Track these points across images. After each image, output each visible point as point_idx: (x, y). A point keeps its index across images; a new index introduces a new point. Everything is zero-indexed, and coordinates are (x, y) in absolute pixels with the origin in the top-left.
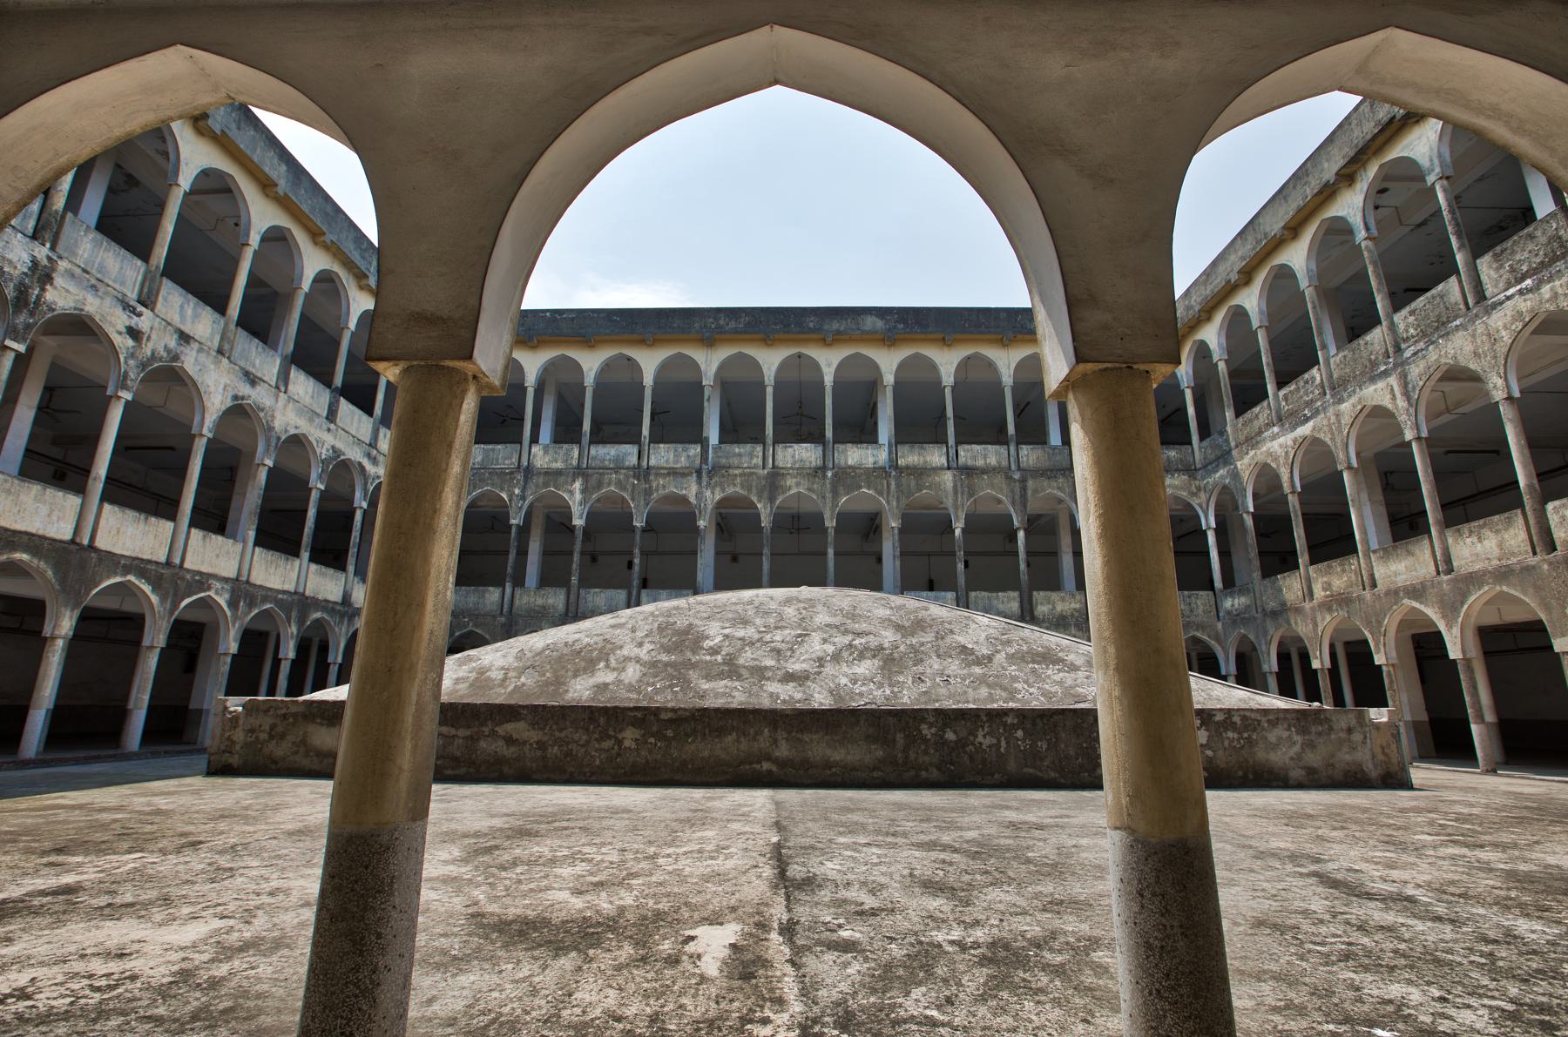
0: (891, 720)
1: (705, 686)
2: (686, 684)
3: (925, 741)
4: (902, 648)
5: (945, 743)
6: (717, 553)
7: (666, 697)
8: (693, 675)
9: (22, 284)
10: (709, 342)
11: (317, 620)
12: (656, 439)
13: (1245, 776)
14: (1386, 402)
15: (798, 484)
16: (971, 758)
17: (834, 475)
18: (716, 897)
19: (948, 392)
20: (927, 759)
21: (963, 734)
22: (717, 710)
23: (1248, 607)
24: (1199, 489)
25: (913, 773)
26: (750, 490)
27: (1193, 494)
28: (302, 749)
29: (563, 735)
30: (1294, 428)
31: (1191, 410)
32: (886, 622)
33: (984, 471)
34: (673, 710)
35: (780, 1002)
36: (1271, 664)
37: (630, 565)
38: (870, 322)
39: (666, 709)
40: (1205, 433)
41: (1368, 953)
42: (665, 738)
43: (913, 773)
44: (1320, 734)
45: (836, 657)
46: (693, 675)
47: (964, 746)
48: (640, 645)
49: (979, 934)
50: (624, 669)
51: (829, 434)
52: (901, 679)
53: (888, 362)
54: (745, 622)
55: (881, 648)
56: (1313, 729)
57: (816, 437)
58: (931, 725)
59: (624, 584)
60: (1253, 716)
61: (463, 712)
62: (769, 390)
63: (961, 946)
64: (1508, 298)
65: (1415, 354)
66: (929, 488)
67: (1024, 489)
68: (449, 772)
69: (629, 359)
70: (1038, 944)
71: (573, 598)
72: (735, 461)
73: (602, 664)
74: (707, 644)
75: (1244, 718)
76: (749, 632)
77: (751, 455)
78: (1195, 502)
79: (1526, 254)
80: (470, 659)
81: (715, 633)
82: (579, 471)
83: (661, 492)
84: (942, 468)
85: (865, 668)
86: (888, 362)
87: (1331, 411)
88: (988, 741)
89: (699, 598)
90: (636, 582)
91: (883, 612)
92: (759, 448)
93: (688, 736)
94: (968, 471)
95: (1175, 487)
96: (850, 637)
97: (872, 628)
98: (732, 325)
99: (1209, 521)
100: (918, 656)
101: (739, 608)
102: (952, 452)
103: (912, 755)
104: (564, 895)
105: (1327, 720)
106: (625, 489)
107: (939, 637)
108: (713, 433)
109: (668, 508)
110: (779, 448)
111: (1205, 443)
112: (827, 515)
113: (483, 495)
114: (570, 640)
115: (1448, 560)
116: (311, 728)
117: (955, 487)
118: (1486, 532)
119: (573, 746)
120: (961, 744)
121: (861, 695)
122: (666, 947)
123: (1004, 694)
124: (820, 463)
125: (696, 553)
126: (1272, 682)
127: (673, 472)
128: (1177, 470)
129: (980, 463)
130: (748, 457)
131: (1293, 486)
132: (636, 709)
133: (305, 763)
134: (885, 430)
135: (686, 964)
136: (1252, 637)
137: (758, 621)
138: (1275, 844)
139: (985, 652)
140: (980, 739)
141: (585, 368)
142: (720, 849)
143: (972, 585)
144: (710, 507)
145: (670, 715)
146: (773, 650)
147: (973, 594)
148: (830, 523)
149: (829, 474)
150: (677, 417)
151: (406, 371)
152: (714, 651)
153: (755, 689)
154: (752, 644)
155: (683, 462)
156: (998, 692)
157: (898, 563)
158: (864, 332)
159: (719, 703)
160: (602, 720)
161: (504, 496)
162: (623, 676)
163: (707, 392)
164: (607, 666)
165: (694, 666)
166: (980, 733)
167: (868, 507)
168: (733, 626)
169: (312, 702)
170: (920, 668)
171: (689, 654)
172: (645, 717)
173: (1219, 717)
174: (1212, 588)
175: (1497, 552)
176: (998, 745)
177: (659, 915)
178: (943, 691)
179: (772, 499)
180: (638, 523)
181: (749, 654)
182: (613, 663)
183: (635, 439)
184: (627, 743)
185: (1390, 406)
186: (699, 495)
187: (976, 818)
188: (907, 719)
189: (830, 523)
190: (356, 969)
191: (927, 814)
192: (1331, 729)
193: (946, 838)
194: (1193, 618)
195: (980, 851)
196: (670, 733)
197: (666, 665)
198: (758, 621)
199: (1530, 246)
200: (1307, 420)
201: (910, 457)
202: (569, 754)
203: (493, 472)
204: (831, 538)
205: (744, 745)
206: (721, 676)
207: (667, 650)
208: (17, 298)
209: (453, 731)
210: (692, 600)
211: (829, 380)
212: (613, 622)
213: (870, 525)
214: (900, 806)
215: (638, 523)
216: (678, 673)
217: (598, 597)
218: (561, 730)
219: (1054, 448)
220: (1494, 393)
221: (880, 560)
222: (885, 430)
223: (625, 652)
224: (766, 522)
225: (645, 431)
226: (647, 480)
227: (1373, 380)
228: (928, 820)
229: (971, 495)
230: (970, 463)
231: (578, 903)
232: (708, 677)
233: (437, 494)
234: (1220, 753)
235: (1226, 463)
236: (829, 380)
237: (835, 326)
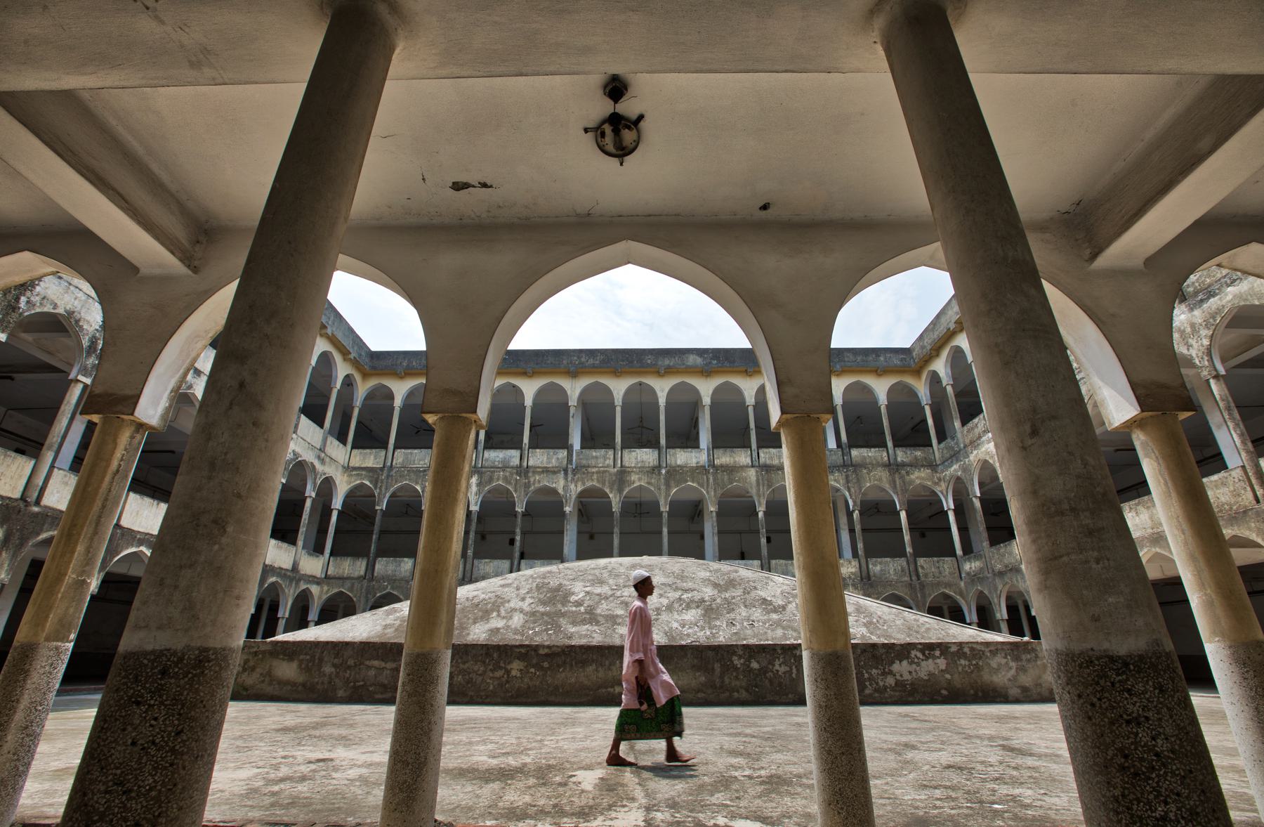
0: (710, 653)
1: (573, 629)
2: (558, 628)
3: (736, 669)
4: (719, 601)
5: (751, 670)
6: (579, 532)
7: (541, 636)
8: (563, 621)
9: (94, 337)
10: (574, 374)
11: (273, 583)
12: (534, 445)
13: (976, 694)
15: (640, 479)
16: (771, 681)
17: (667, 472)
18: (586, 758)
19: (751, 410)
20: (738, 683)
21: (764, 664)
22: (581, 647)
23: (981, 569)
24: (940, 480)
25: (727, 694)
26: (604, 484)
27: (936, 484)
28: (267, 679)
29: (466, 666)
31: (930, 422)
32: (706, 581)
34: (548, 647)
35: (633, 799)
36: (1002, 613)
37: (512, 542)
38: (692, 360)
39: (544, 647)
40: (942, 437)
41: (1012, 777)
42: (542, 668)
43: (727, 694)
44: (1029, 661)
45: (670, 608)
46: (563, 621)
47: (765, 673)
48: (523, 599)
49: (763, 773)
50: (511, 618)
51: (663, 441)
52: (718, 623)
53: (706, 388)
54: (601, 582)
55: (703, 601)
56: (1024, 657)
57: (653, 444)
58: (740, 657)
59: (509, 557)
60: (978, 647)
61: (391, 649)
62: (618, 409)
63: (750, 777)
66: (738, 481)
68: (379, 696)
69: (514, 386)
70: (799, 776)
71: (469, 566)
72: (593, 462)
73: (495, 614)
74: (573, 598)
75: (972, 649)
76: (604, 590)
77: (605, 458)
78: (937, 489)
80: (395, 611)
81: (579, 590)
84: (747, 466)
85: (691, 615)
86: (706, 388)
88: (783, 669)
89: (566, 565)
90: (517, 554)
91: (704, 574)
92: (611, 453)
93: (559, 666)
96: (679, 593)
97: (696, 586)
98: (591, 361)
99: (949, 504)
100: (730, 606)
101: (597, 572)
102: (755, 454)
103: (727, 680)
104: (485, 758)
105: (1034, 650)
106: (510, 483)
107: (746, 592)
108: (576, 440)
109: (542, 498)
110: (626, 452)
111: (942, 445)
112: (662, 502)
113: (401, 488)
114: (471, 595)
116: (275, 663)
117: (758, 481)
119: (473, 676)
120: (763, 671)
121: (688, 635)
122: (558, 779)
123: (795, 634)
124: (656, 463)
125: (562, 533)
126: (1004, 626)
127: (546, 471)
129: (776, 462)
130: (602, 459)
132: (521, 646)
133: (269, 690)
134: (705, 438)
135: (571, 785)
136: (986, 592)
137: (611, 582)
138: (982, 732)
139: (781, 603)
140: (777, 667)
142: (586, 737)
143: (772, 556)
144: (574, 497)
145: (546, 651)
146: (622, 603)
147: (773, 562)
148: (664, 508)
149: (663, 471)
150: (549, 431)
151: (441, 418)
152: (579, 604)
153: (609, 632)
154: (606, 598)
155: (554, 463)
156: (790, 632)
157: (716, 539)
158: (688, 367)
159: (583, 642)
160: (495, 655)
161: (418, 488)
162: (510, 623)
163: (572, 411)
164: (499, 615)
165: (563, 615)
166: (777, 663)
167: (693, 497)
168: (593, 585)
169: (277, 642)
170: (732, 615)
171: (559, 606)
172: (527, 653)
173: (954, 649)
174: (953, 554)
175: (1149, 523)
176: (790, 672)
177: (549, 767)
178: (749, 632)
179: (620, 491)
180: (520, 509)
181: (604, 606)
182: (503, 613)
183: (517, 445)
184: (514, 673)
187: (772, 721)
188: (722, 653)
189: (664, 508)
190: (422, 721)
191: (737, 719)
192: (1037, 657)
193: (748, 731)
194: (942, 579)
195: (769, 738)
196: (546, 665)
197: (543, 614)
198: (611, 582)
201: (723, 458)
202: (470, 681)
203: (411, 471)
205: (601, 674)
206: (584, 622)
207: (544, 603)
208: (90, 347)
209: (383, 665)
210: (561, 566)
211: (662, 401)
212: (503, 582)
213: (691, 512)
214: (717, 715)
215: (520, 509)
216: (552, 620)
217: (486, 565)
218: (464, 663)
219: (831, 450)
221: (702, 537)
222: (705, 438)
223: (512, 605)
224: (616, 507)
225: (526, 440)
226: (527, 477)
228: (737, 722)
229: (769, 486)
230: (768, 462)
231: (494, 762)
232: (574, 623)
233: (459, 481)
234: (956, 676)
235: (958, 460)
236: (662, 401)
237: (667, 362)
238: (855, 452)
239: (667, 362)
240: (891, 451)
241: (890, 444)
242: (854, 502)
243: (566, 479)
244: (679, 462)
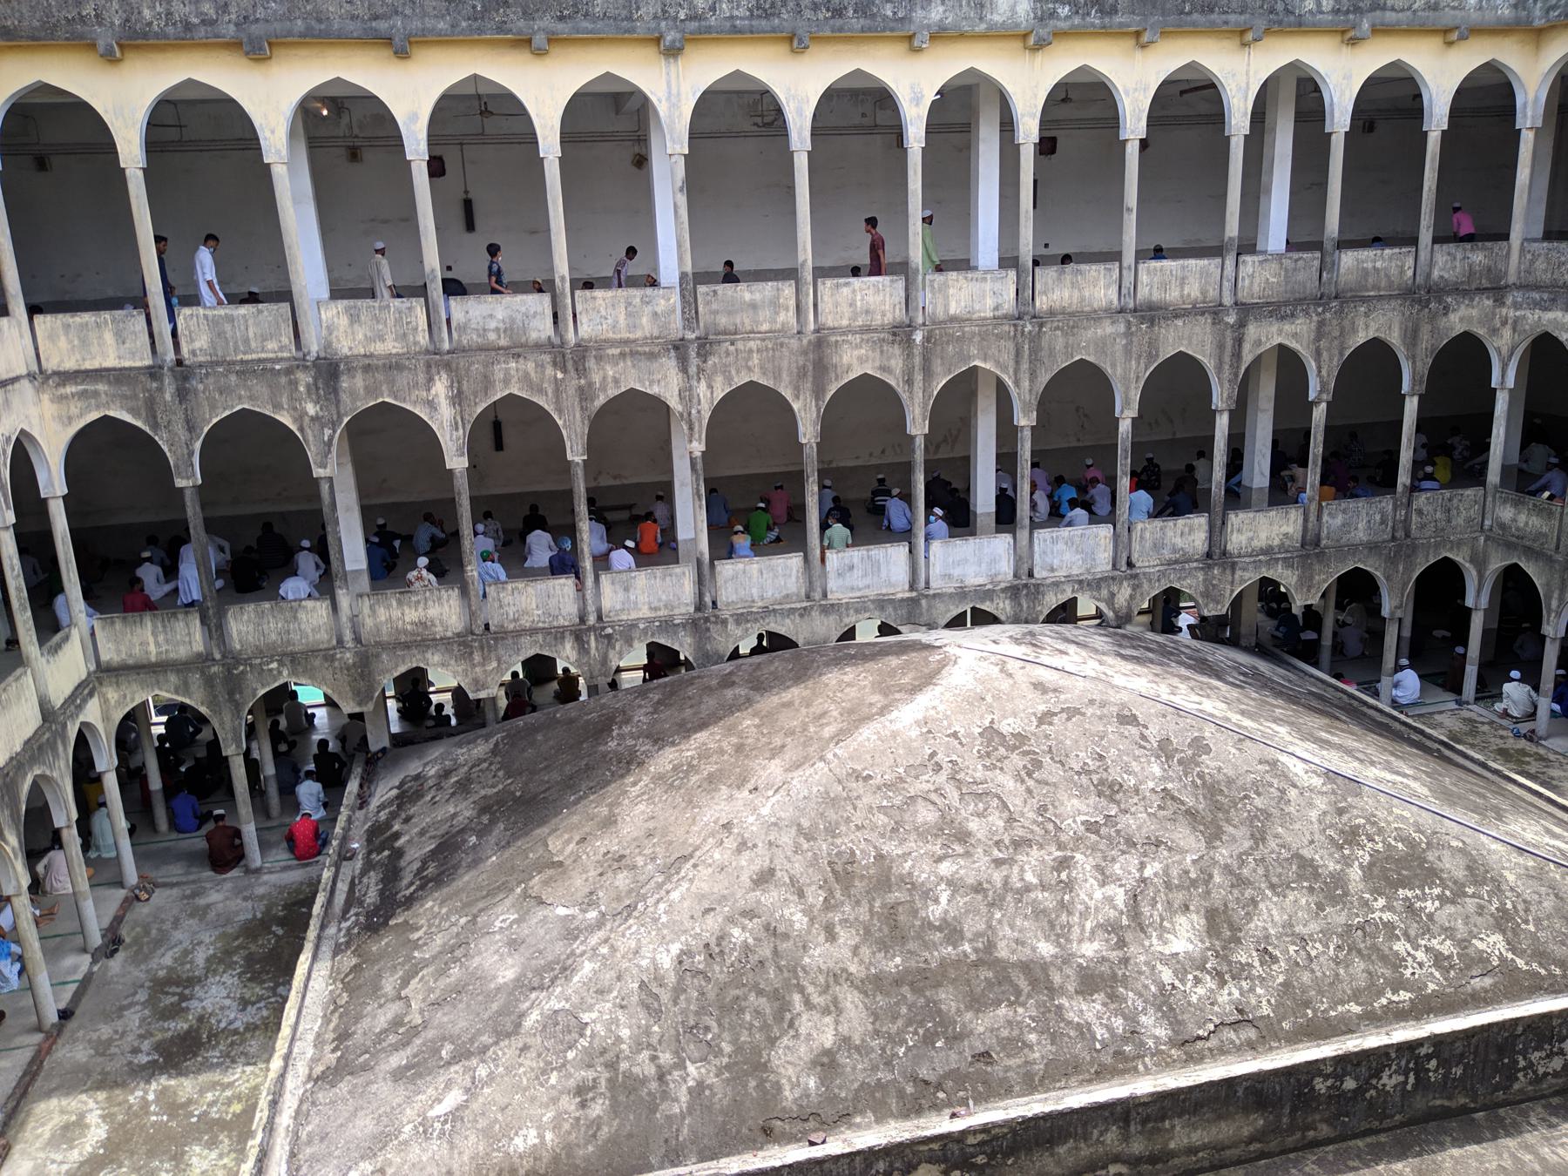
17: (927, 339)
25: (1298, 1135)
26: (777, 376)
33: (1179, 313)
67: (1239, 342)
72: (744, 320)
77: (775, 305)
82: (436, 360)
83: (612, 392)
94: (1152, 314)
95: (1470, 319)
102: (1128, 278)
106: (541, 391)
124: (899, 314)
127: (631, 350)
129: (1173, 295)
140: (1385, 1080)
141: (399, 112)
144: (707, 415)
145: (980, 1137)
149: (918, 337)
158: (992, 26)
161: (285, 419)
166: (1385, 1075)
176: (1406, 1082)
186: (686, 394)
204: (919, 456)
205: (1085, 1151)
226: (581, 371)
238: (1348, 259)
240: (1424, 255)
241: (1426, 236)
243: (684, 369)
244: (954, 309)
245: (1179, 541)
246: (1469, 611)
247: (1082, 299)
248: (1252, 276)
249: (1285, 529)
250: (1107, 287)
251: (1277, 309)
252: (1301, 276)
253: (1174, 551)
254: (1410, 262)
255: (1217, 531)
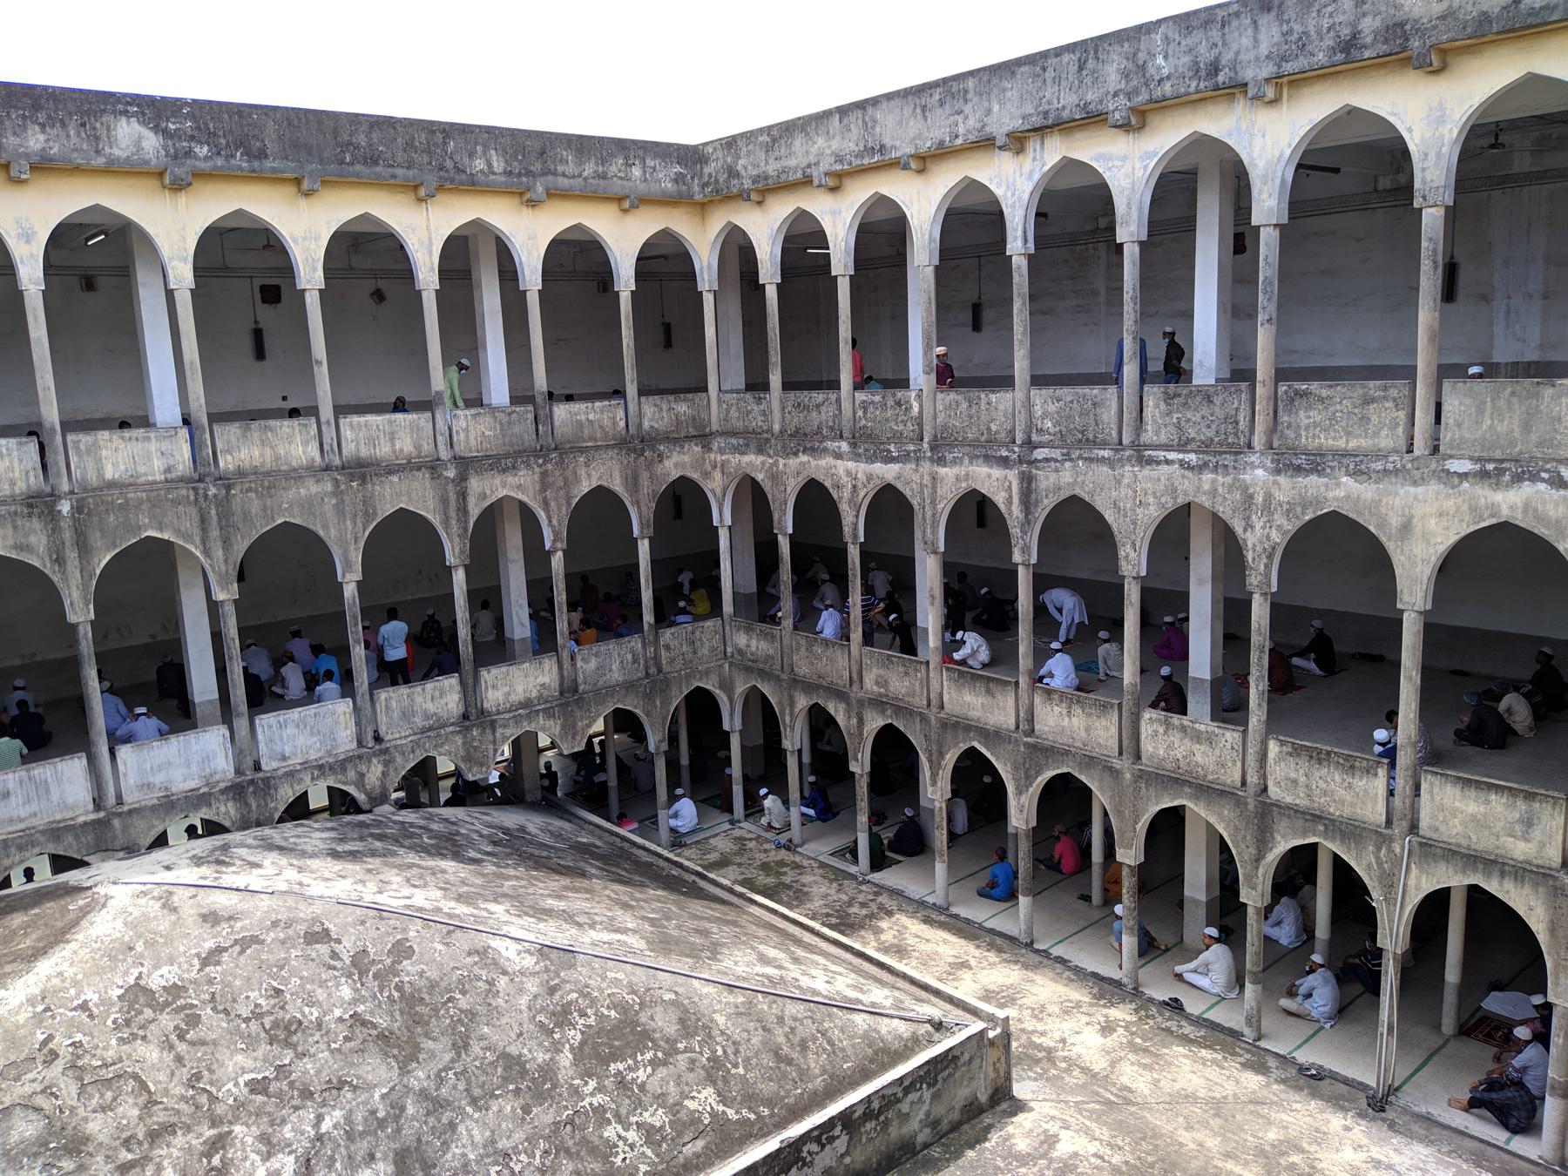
14: (999, 499)
17: (78, 509)
30: (871, 459)
33: (391, 469)
64: (1167, 462)
65: (1047, 460)
67: (463, 495)
79: (1197, 418)
87: (926, 466)
94: (361, 470)
115: (1031, 720)
118: (1077, 710)
124: (36, 481)
128: (689, 438)
129: (383, 451)
131: (855, 536)
149: (65, 507)
185: (1002, 507)
199: (1205, 411)
200: (890, 459)
201: (241, 450)
204: (87, 646)
220: (1123, 563)
227: (988, 459)
230: (365, 452)
238: (561, 411)
239: (35, 140)
240: (632, 407)
241: (631, 390)
242: (556, 534)
244: (109, 473)
245: (430, 707)
246: (728, 733)
247: (277, 458)
248: (467, 430)
249: (541, 680)
250: (305, 443)
251: (498, 462)
252: (516, 429)
253: (427, 717)
254: (621, 414)
255: (470, 691)
